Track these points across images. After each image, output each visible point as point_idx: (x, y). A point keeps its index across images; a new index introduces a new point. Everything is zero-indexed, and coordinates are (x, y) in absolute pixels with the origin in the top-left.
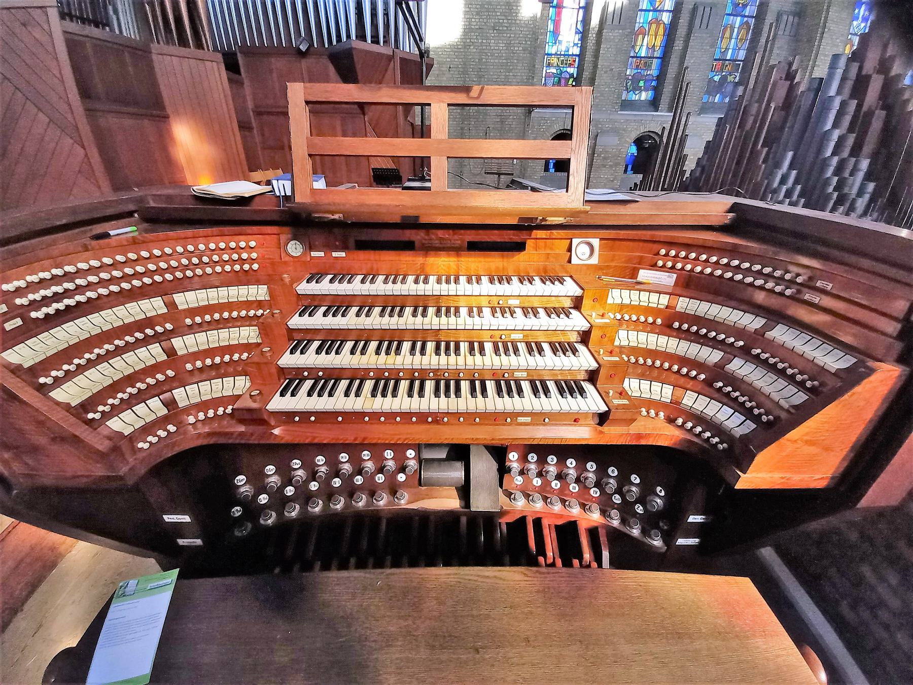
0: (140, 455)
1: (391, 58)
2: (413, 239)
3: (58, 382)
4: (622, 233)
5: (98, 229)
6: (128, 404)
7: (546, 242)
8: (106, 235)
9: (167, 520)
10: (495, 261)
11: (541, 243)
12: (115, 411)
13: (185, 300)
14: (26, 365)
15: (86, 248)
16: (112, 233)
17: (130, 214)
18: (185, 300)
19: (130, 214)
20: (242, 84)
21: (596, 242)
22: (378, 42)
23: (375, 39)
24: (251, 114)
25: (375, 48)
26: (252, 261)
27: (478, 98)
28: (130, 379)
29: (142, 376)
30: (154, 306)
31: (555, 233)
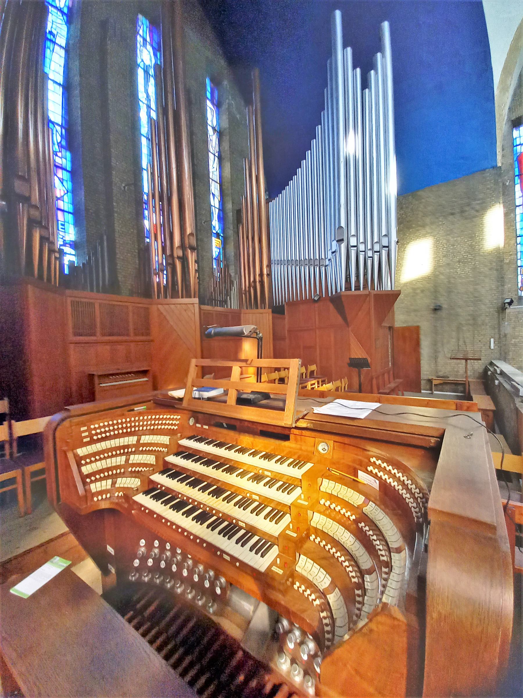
0: (92, 503)
1: (367, 296)
2: (236, 424)
3: (87, 463)
4: (346, 440)
5: (132, 407)
6: (101, 479)
7: (301, 438)
8: (133, 410)
9: (113, 550)
10: (271, 444)
11: (299, 437)
12: (96, 480)
13: (145, 439)
14: (81, 455)
15: (123, 415)
16: (135, 409)
17: (150, 401)
18: (145, 439)
19: (150, 401)
20: (285, 318)
21: (331, 443)
22: (359, 289)
23: (357, 288)
24: (286, 332)
25: (357, 292)
26: (175, 425)
27: (250, 364)
28: (108, 469)
29: (113, 469)
30: (132, 440)
31: (304, 432)
